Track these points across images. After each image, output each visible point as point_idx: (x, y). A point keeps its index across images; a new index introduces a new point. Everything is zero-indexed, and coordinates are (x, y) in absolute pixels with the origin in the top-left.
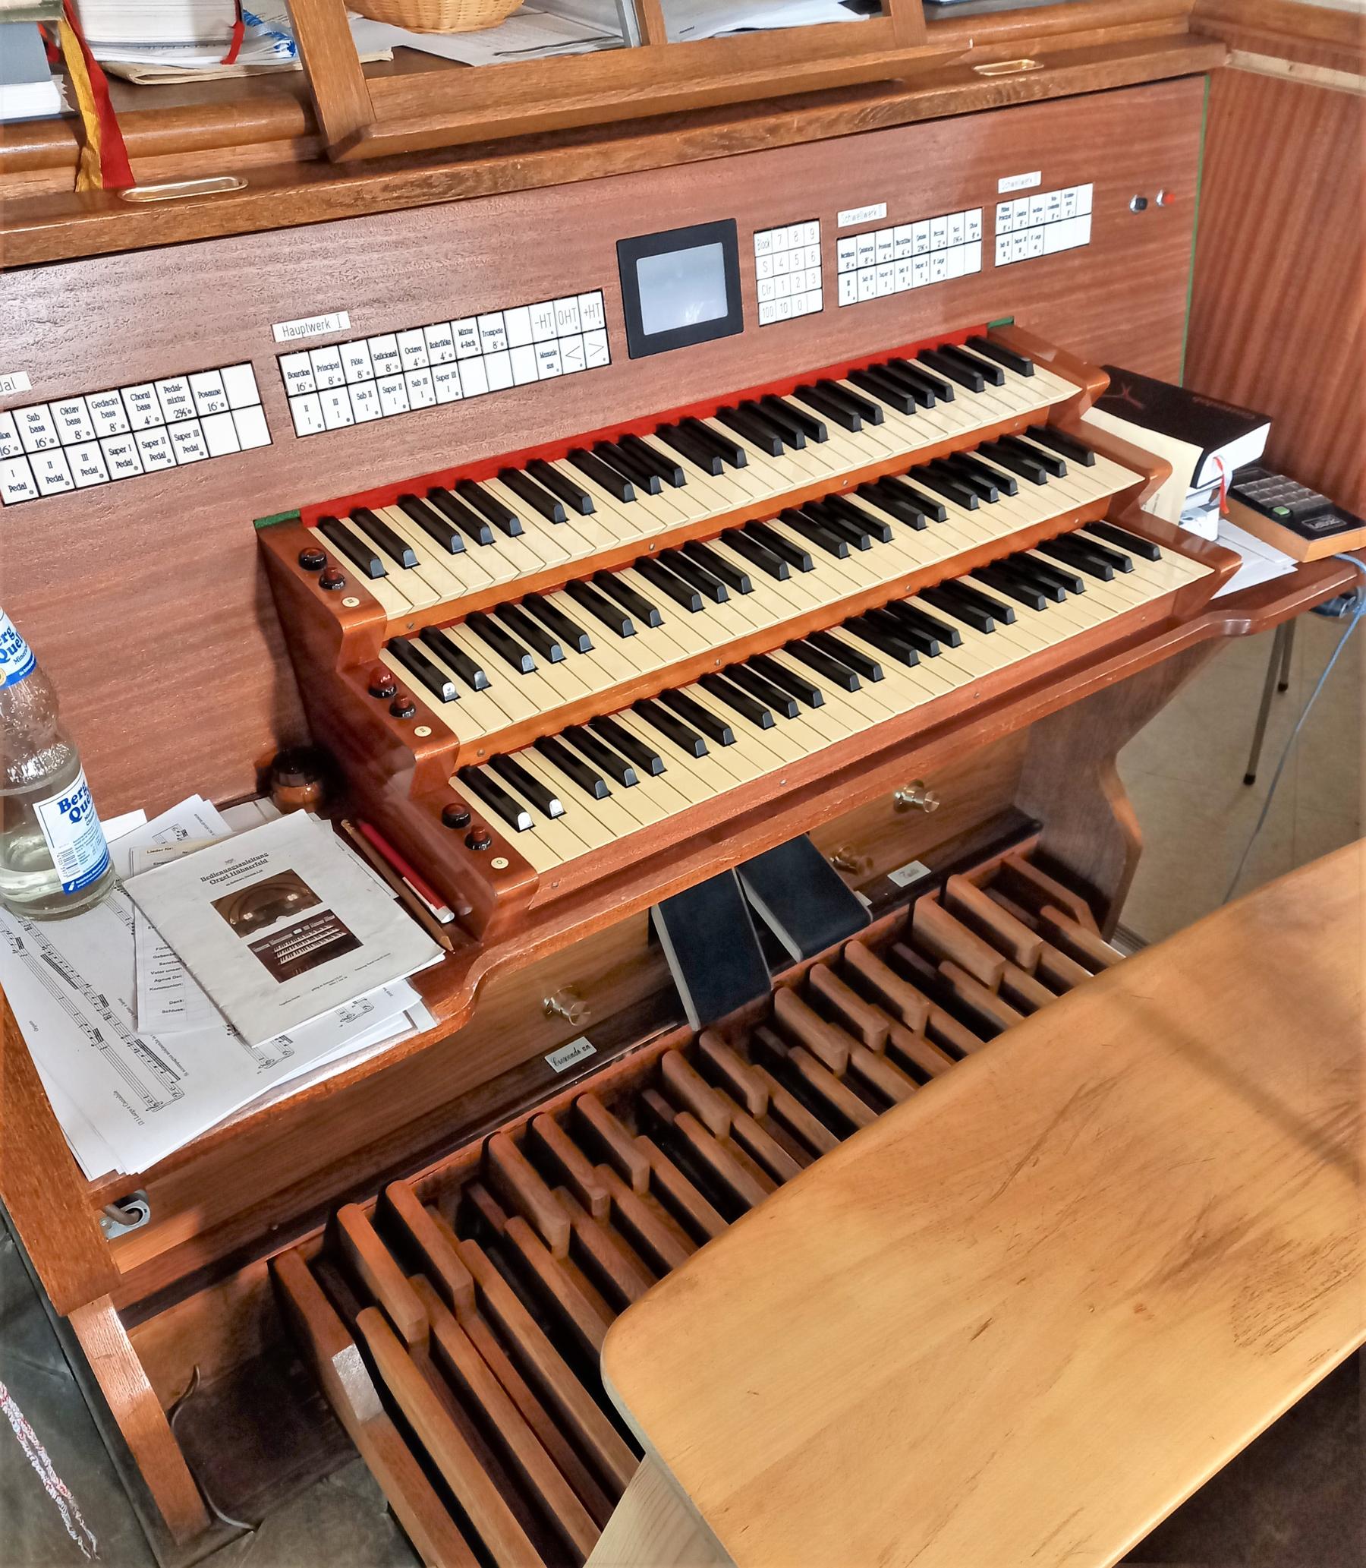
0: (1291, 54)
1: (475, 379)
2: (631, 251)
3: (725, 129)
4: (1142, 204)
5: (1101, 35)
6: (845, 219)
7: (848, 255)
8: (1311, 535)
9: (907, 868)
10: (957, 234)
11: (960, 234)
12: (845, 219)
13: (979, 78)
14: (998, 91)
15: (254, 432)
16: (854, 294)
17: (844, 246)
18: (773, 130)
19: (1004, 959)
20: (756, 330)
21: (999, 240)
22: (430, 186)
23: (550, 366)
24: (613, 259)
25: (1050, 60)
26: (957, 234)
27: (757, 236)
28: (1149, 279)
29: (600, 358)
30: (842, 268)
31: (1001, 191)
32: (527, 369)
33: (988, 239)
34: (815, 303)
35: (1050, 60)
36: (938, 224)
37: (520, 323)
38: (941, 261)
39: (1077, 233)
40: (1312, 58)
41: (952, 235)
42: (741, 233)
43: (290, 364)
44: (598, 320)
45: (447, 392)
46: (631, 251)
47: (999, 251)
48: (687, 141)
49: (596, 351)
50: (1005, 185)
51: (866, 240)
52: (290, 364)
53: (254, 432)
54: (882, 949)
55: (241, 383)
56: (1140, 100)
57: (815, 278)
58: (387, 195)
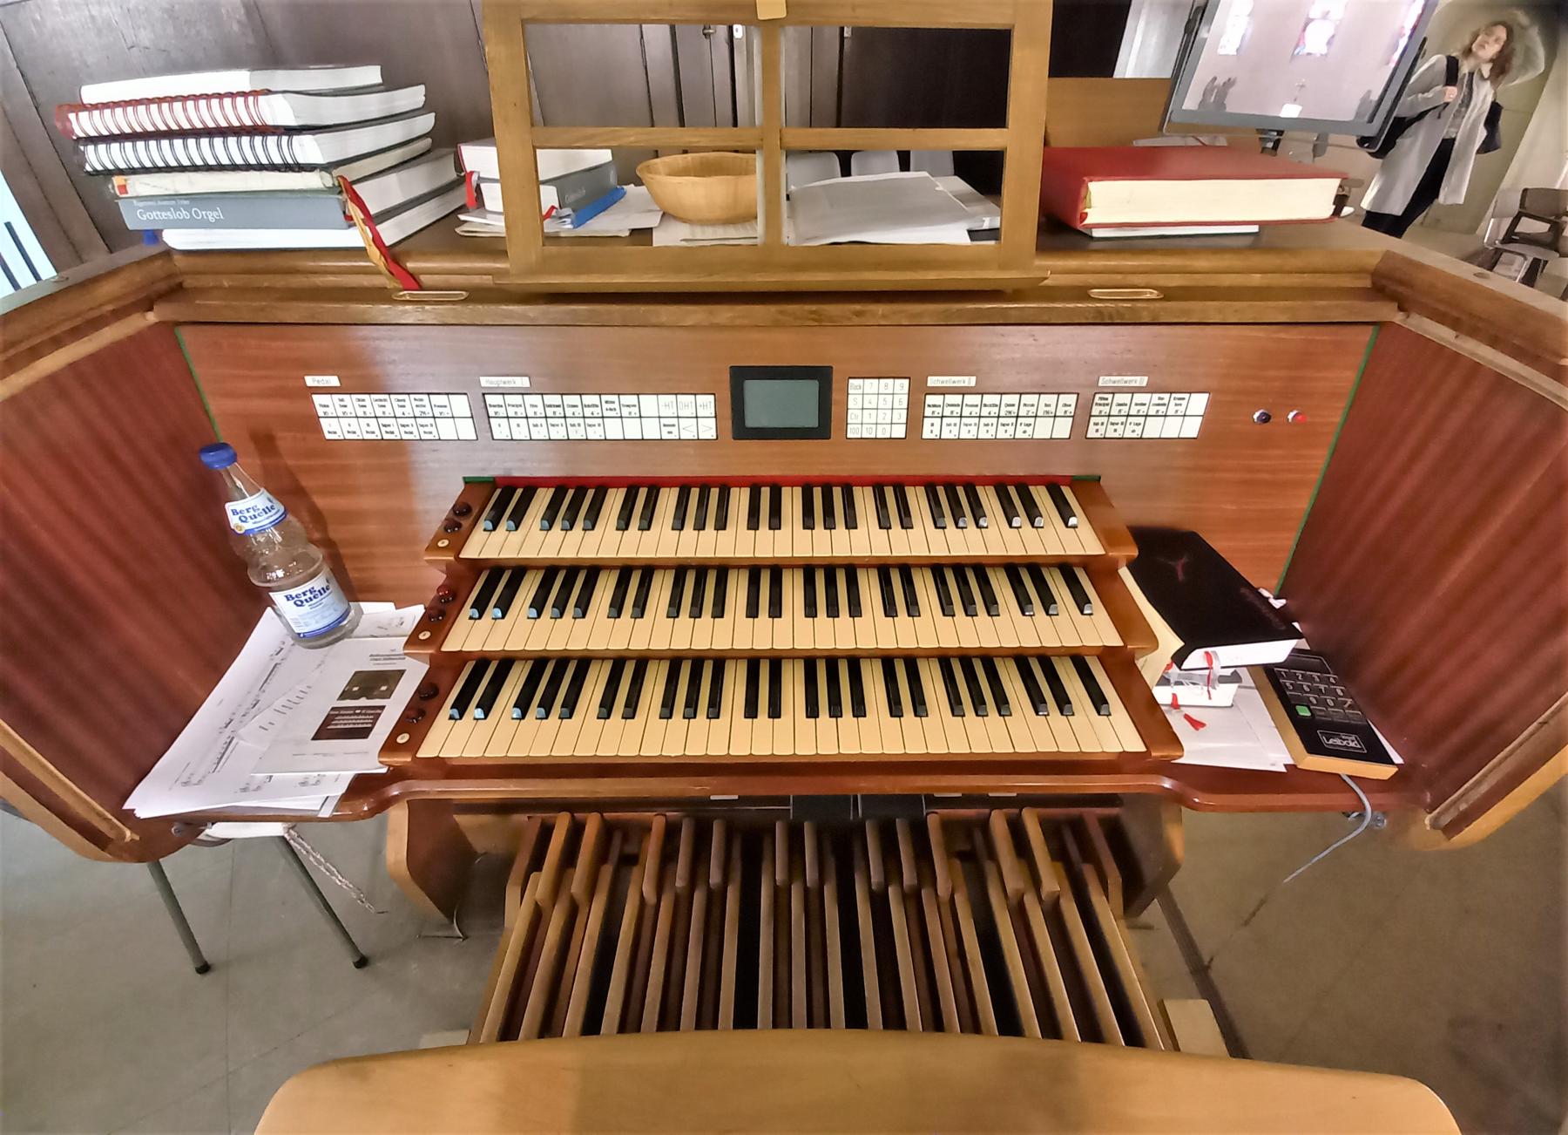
0: (1455, 324)
1: (614, 431)
2: (740, 375)
3: (814, 307)
4: (1266, 418)
5: (1256, 280)
6: (933, 381)
8: (1314, 747)
12: (933, 381)
13: (1090, 298)
14: (1099, 311)
15: (467, 431)
18: (858, 314)
21: (1093, 420)
25: (1168, 294)
28: (1266, 476)
30: (928, 412)
32: (652, 431)
34: (899, 432)
37: (649, 403)
39: (1192, 429)
40: (1473, 333)
42: (835, 377)
43: (490, 399)
44: (711, 411)
45: (595, 433)
47: (1092, 428)
48: (781, 312)
49: (708, 430)
52: (490, 399)
53: (467, 431)
55: (460, 404)
56: (1283, 335)
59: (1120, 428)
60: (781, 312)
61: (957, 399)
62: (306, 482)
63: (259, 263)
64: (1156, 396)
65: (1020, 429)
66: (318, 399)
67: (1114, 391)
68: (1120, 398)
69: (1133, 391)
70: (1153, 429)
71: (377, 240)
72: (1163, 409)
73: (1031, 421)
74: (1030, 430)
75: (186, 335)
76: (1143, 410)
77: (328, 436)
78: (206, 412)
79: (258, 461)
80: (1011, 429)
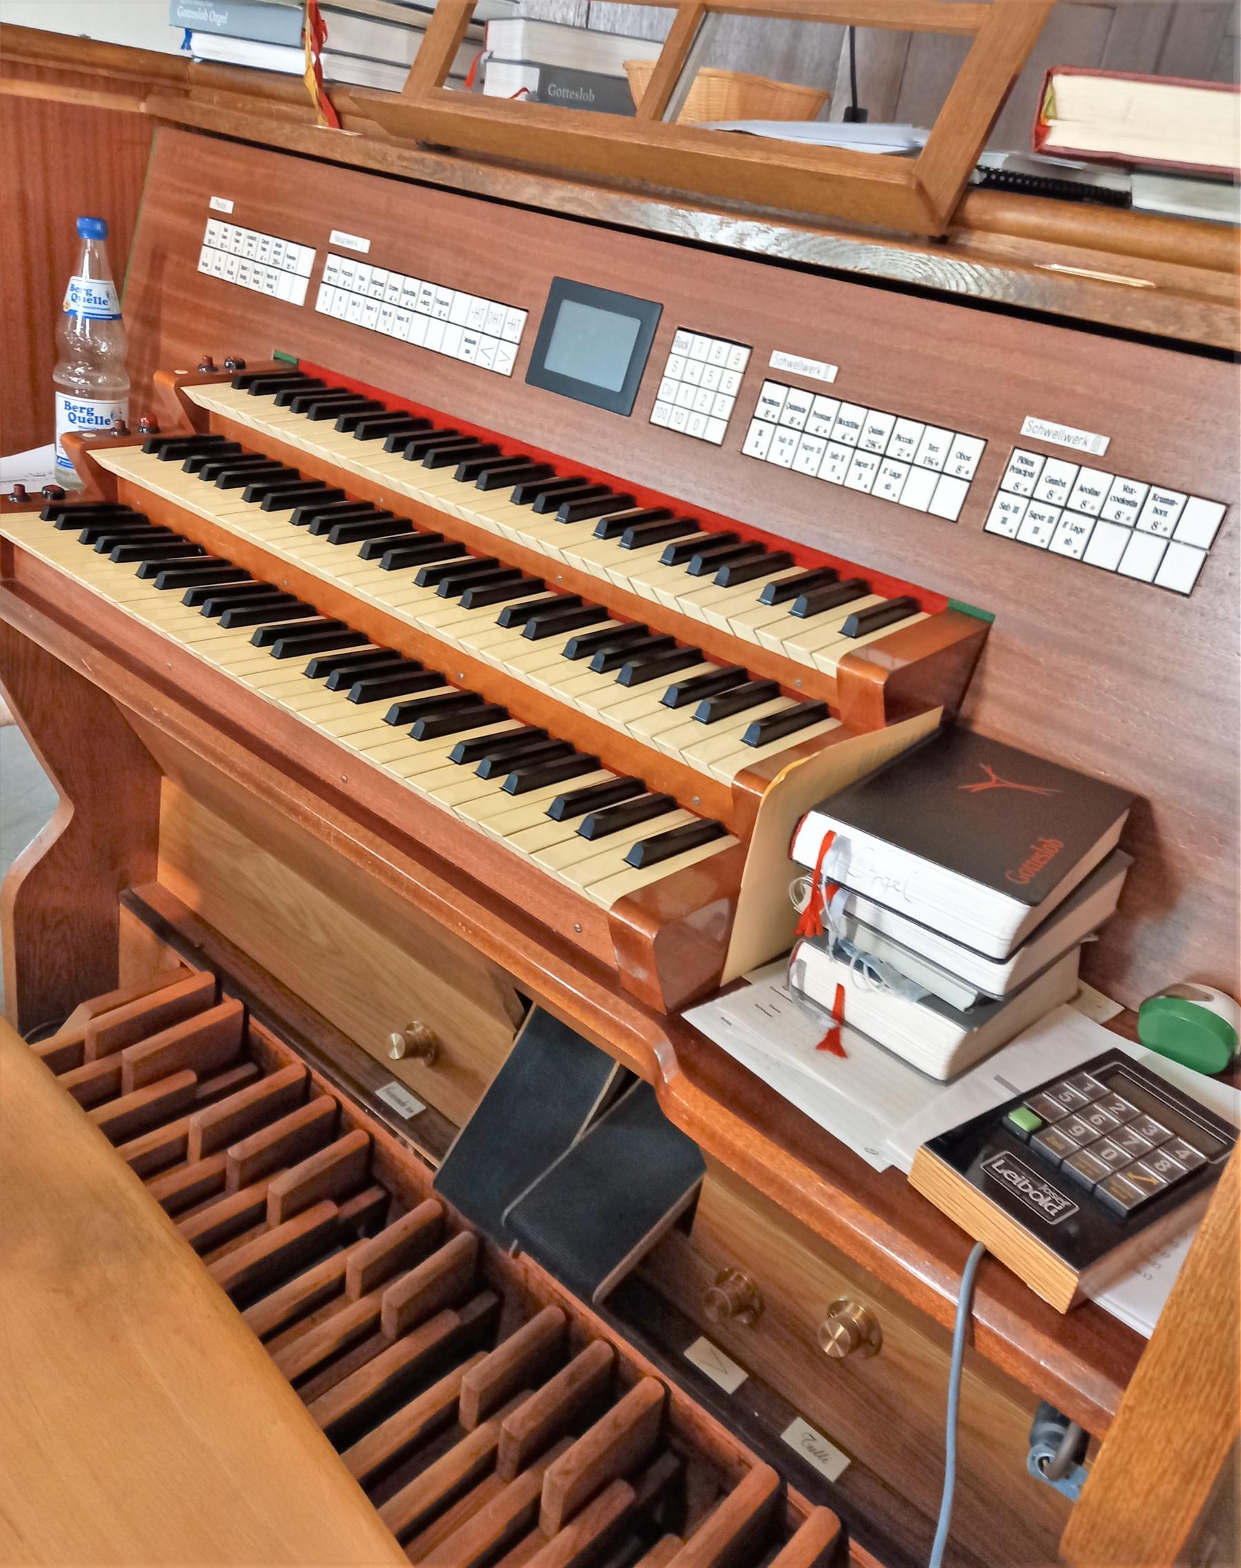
2: (563, 290)
6: (780, 360)
7: (771, 402)
9: (822, 1443)
10: (932, 454)
11: (939, 457)
12: (780, 360)
16: (763, 447)
20: (643, 423)
21: (1002, 497)
22: (424, 164)
23: (468, 352)
24: (546, 291)
26: (932, 454)
27: (680, 333)
29: (505, 367)
31: (1025, 431)
33: (983, 489)
36: (907, 428)
38: (896, 476)
41: (924, 453)
44: (515, 335)
46: (563, 290)
49: (502, 358)
50: (1033, 427)
51: (801, 398)
57: (725, 407)
59: (1046, 529)
60: (642, 222)
62: (166, 315)
64: (1120, 482)
65: (884, 479)
66: (212, 224)
67: (1048, 451)
68: (1056, 468)
69: (1082, 460)
70: (1104, 550)
71: (318, 68)
72: (1132, 512)
74: (897, 484)
75: (162, 138)
76: (1094, 504)
77: (201, 268)
78: (136, 216)
79: (144, 281)
80: (869, 475)
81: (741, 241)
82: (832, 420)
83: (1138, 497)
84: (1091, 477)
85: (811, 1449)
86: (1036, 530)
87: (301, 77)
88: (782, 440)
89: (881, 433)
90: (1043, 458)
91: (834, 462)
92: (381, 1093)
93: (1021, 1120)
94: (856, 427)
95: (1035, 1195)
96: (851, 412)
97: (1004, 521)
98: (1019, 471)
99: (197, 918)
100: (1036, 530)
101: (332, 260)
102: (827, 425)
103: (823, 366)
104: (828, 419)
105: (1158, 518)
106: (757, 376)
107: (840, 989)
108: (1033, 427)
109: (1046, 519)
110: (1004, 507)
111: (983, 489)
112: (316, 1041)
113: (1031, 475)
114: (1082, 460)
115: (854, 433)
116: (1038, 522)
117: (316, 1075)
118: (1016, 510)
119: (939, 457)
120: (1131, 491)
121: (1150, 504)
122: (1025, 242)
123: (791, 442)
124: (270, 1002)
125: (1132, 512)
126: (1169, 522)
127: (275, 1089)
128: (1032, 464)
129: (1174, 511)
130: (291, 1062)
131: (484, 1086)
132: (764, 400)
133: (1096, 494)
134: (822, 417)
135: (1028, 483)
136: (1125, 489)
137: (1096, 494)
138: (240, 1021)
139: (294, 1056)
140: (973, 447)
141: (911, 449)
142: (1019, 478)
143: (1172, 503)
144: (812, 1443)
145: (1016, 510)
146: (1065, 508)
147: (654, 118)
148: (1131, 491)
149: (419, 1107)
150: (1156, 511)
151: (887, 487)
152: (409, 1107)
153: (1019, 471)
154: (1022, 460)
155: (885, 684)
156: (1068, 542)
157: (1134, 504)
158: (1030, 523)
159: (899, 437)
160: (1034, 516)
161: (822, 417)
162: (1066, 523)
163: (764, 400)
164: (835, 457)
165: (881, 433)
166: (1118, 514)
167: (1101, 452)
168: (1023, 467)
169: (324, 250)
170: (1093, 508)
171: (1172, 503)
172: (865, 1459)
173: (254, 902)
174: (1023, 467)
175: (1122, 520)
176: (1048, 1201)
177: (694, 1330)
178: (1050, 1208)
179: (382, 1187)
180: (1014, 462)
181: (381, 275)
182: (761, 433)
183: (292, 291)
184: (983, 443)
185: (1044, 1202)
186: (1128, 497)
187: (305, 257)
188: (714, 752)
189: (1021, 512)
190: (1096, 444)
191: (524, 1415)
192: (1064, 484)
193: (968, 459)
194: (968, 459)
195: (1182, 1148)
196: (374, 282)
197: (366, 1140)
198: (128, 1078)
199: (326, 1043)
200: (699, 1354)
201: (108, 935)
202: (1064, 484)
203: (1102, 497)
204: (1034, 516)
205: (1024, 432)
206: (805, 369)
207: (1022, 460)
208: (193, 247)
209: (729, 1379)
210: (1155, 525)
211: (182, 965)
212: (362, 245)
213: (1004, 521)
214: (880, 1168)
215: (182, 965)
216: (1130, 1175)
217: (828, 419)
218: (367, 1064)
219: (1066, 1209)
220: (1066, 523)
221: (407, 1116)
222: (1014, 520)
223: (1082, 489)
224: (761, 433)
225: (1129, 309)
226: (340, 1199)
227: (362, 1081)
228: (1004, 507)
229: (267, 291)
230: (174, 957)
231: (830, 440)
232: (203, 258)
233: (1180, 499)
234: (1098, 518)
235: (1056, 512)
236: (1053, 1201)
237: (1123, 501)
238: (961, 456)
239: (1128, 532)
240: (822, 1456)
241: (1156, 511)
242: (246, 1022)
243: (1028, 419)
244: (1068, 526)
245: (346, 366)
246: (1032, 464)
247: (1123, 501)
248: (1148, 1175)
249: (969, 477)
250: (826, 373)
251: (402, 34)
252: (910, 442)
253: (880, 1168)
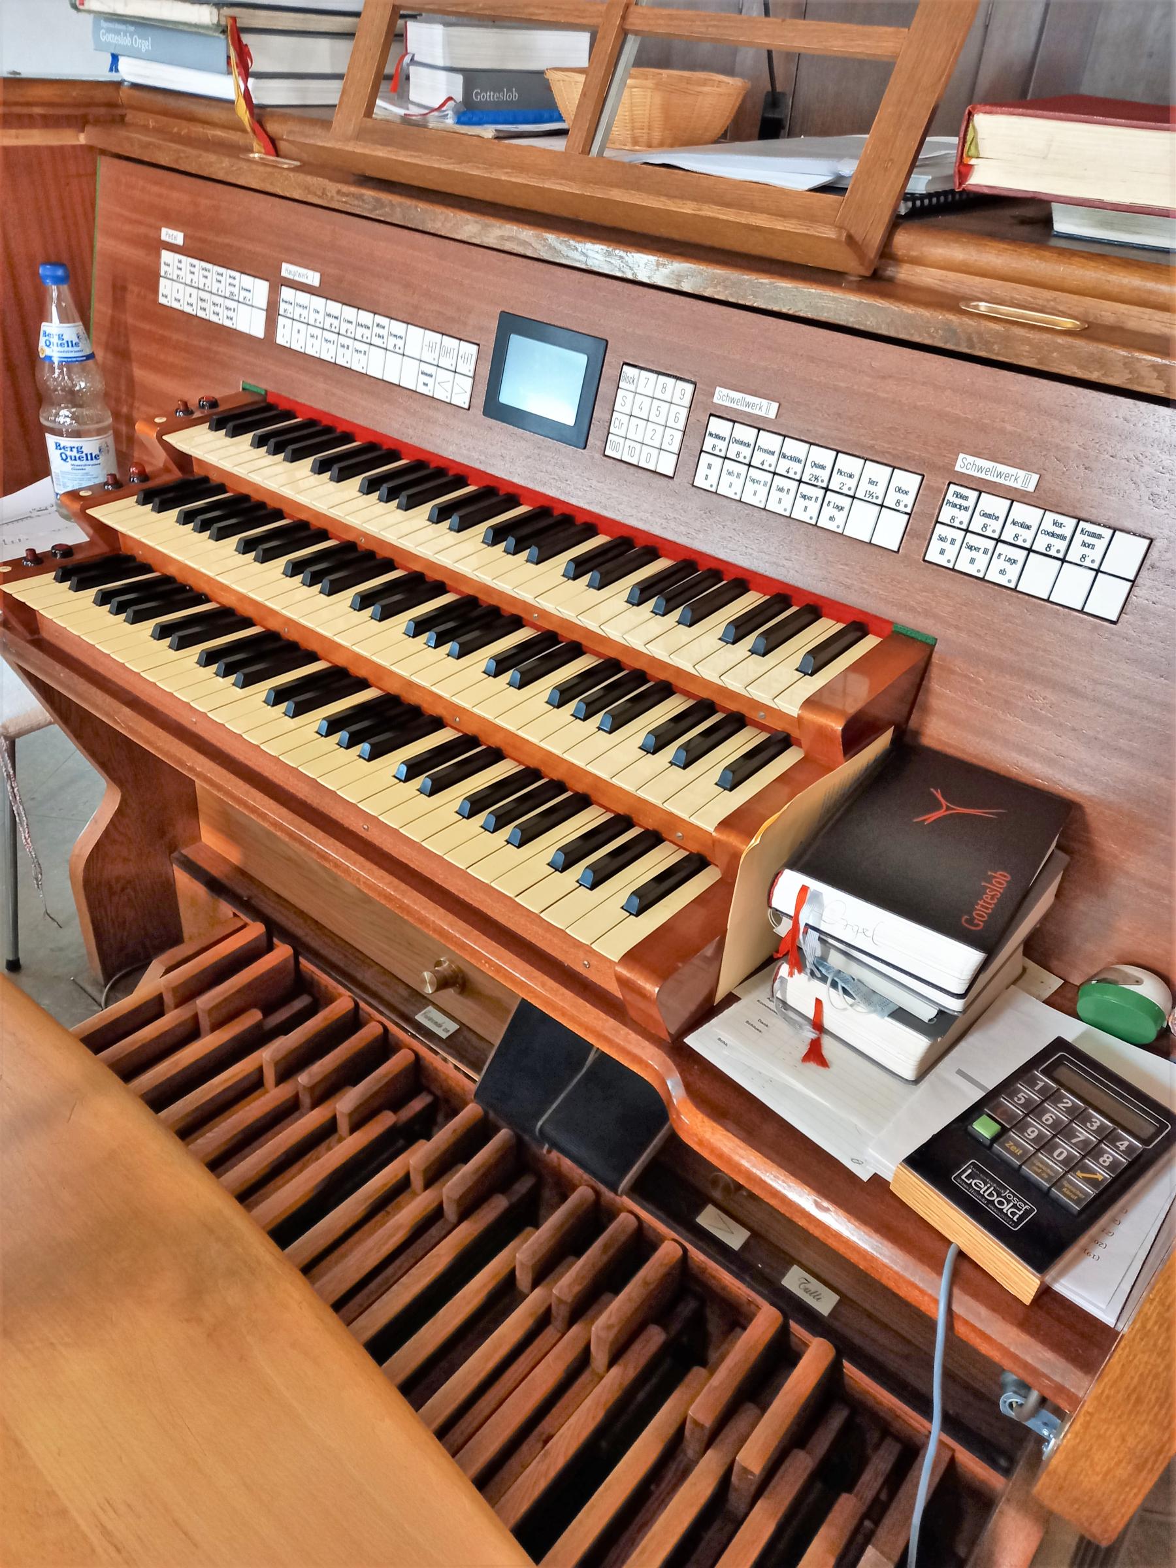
6: (723, 397)
7: (717, 437)
9: (815, 1284)
10: (872, 488)
12: (723, 397)
17: (717, 426)
19: (870, 1546)
20: (598, 456)
24: (494, 325)
25: (1090, 331)
26: (872, 488)
29: (462, 400)
35: (1090, 331)
44: (468, 368)
46: (512, 324)
50: (966, 464)
54: (951, 1482)
57: (674, 441)
58: (339, 198)
61: (748, 434)
62: (135, 347)
63: (172, 103)
66: (166, 256)
67: (982, 487)
68: (989, 503)
69: (1014, 496)
70: (1037, 579)
71: (247, 96)
73: (845, 502)
74: (840, 517)
75: (105, 168)
76: (1026, 537)
77: (162, 300)
78: (92, 247)
79: (110, 311)
80: (814, 507)
81: (679, 282)
82: (777, 454)
83: (1068, 532)
84: (1021, 511)
85: (806, 1290)
86: (972, 561)
87: (232, 102)
88: (730, 473)
89: (823, 467)
90: (976, 494)
91: (780, 495)
92: (419, 1017)
93: (984, 1128)
94: (799, 461)
95: (1001, 1203)
96: (794, 448)
97: (942, 552)
98: (955, 506)
99: (241, 872)
100: (972, 561)
101: (286, 293)
102: (772, 460)
103: (765, 402)
104: (773, 453)
105: (1086, 551)
106: (702, 413)
107: (818, 1003)
108: (966, 464)
109: (982, 551)
110: (942, 539)
111: (921, 523)
112: (359, 976)
113: (966, 509)
114: (1014, 496)
115: (798, 467)
116: (974, 554)
117: (362, 1004)
118: (953, 542)
119: (879, 491)
120: (1060, 525)
121: (1079, 538)
122: (951, 275)
123: (739, 476)
124: (315, 944)
125: (1062, 545)
126: (1096, 554)
127: (329, 1022)
128: (966, 498)
129: (1101, 545)
130: (340, 995)
131: (508, 1011)
132: (711, 434)
133: (1028, 527)
134: (766, 451)
135: (964, 516)
136: (1055, 523)
137: (1028, 527)
138: (292, 962)
139: (341, 989)
140: (911, 482)
141: (852, 483)
142: (955, 512)
143: (1099, 536)
144: (808, 1286)
145: (953, 542)
146: (998, 540)
147: (583, 152)
148: (1060, 525)
149: (453, 1027)
150: (1084, 544)
151: (832, 518)
152: (445, 1027)
153: (955, 506)
154: (958, 495)
155: (843, 730)
156: (1002, 572)
157: (1063, 538)
158: (966, 554)
159: (840, 472)
160: (970, 548)
161: (766, 451)
162: (1000, 555)
163: (711, 434)
164: (780, 490)
165: (823, 467)
166: (1049, 546)
167: (1031, 488)
168: (958, 501)
169: (277, 283)
170: (1025, 541)
171: (1099, 536)
172: (851, 1294)
173: (289, 859)
174: (958, 501)
175: (1053, 552)
176: (1012, 1207)
177: (701, 1201)
178: (1013, 1214)
179: (430, 1092)
180: (949, 496)
181: (334, 307)
182: (709, 466)
183: (252, 323)
184: (920, 477)
185: (1006, 1208)
186: (1058, 531)
187: (261, 289)
188: (695, 796)
189: (958, 543)
190: (1026, 481)
191: (569, 1281)
192: (997, 518)
193: (906, 493)
194: (906, 493)
195: (1122, 1139)
196: (329, 315)
197: (412, 1057)
198: (205, 1023)
199: (367, 976)
200: (708, 1219)
201: (168, 890)
202: (997, 518)
203: (1034, 529)
204: (970, 548)
205: (957, 468)
206: (748, 405)
207: (958, 495)
208: (151, 279)
209: (735, 1238)
210: (1084, 557)
211: (235, 915)
212: (313, 278)
213: (942, 552)
214: (865, 1177)
215: (235, 915)
216: (1079, 1173)
217: (773, 453)
218: (405, 993)
219: (1027, 1213)
220: (1000, 555)
221: (444, 1035)
222: (951, 551)
223: (1014, 523)
224: (709, 466)
225: (1055, 354)
226: (395, 1111)
227: (402, 1008)
228: (942, 539)
229: (228, 323)
230: (226, 909)
231: (775, 473)
232: (162, 290)
233: (1107, 533)
234: (1030, 550)
235: (990, 544)
236: (1015, 1206)
237: (1053, 535)
238: (899, 490)
239: (1059, 563)
240: (816, 1295)
241: (1084, 544)
242: (297, 962)
243: (961, 456)
244: (1003, 557)
245: (315, 397)
246: (966, 498)
247: (1053, 535)
248: (1094, 1172)
249: (908, 510)
250: (768, 409)
251: (324, 44)
252: (851, 476)
253: (865, 1177)
